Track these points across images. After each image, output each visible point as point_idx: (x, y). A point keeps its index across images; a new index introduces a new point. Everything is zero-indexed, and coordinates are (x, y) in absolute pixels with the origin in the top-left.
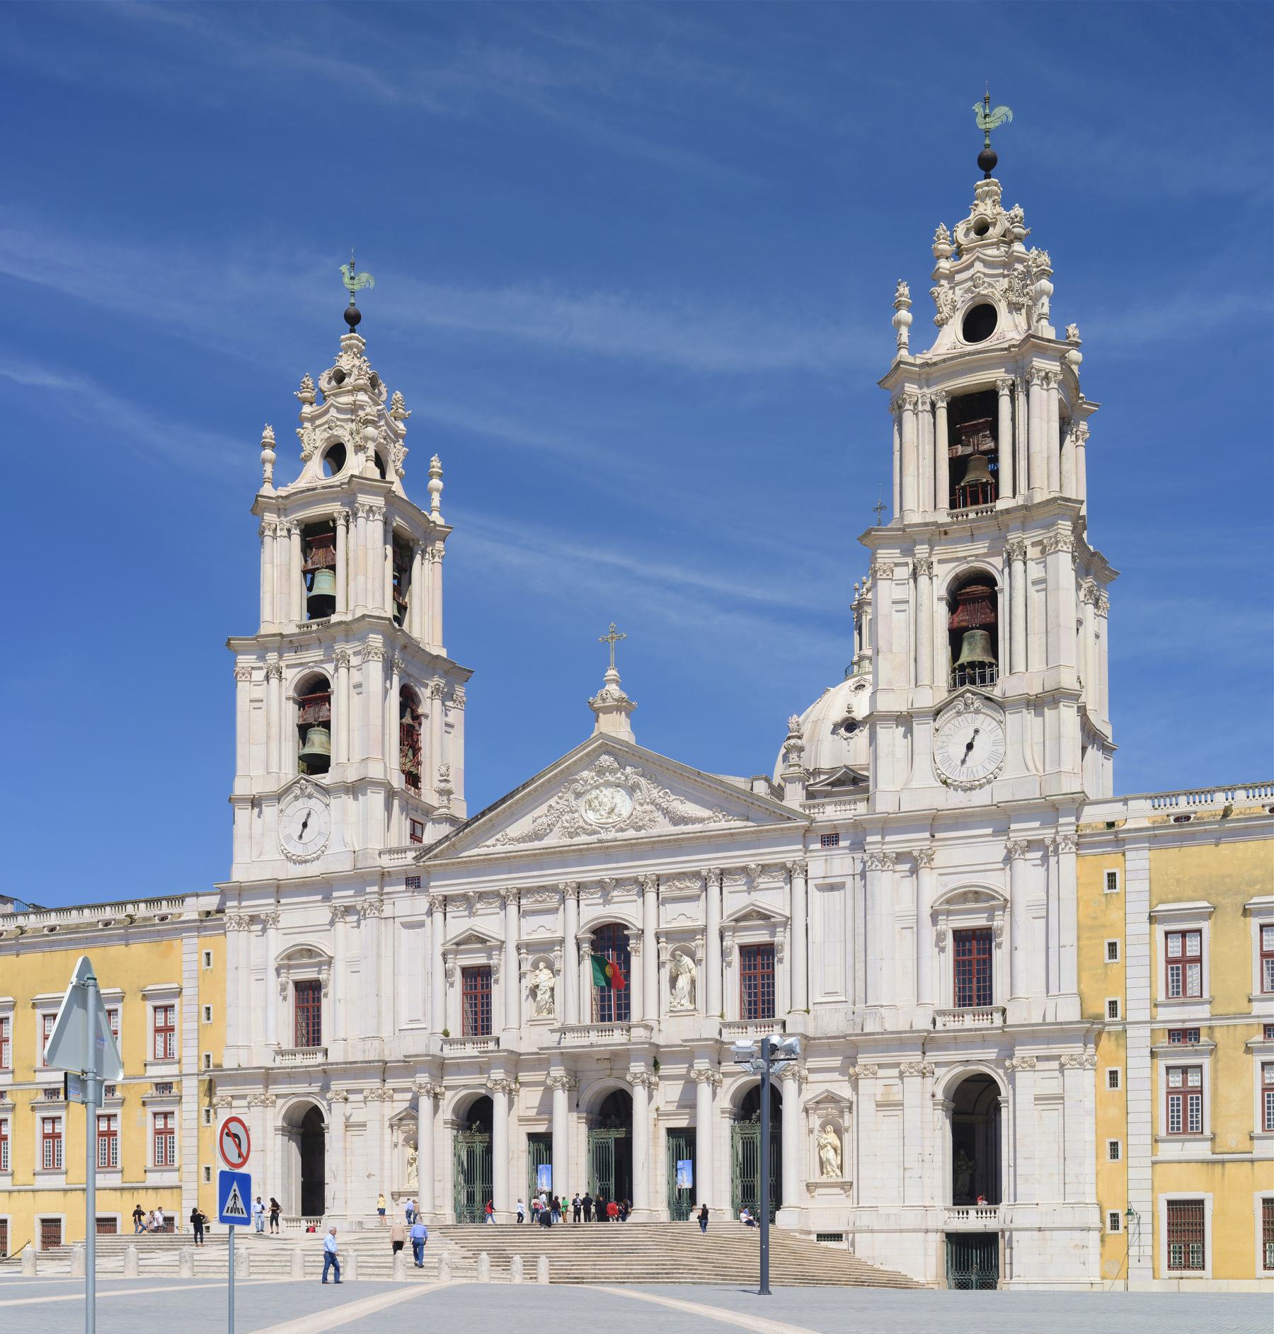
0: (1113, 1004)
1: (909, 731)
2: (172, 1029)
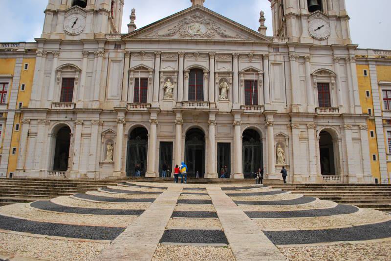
0: (370, 110)
1: (301, 19)
2: (6, 92)
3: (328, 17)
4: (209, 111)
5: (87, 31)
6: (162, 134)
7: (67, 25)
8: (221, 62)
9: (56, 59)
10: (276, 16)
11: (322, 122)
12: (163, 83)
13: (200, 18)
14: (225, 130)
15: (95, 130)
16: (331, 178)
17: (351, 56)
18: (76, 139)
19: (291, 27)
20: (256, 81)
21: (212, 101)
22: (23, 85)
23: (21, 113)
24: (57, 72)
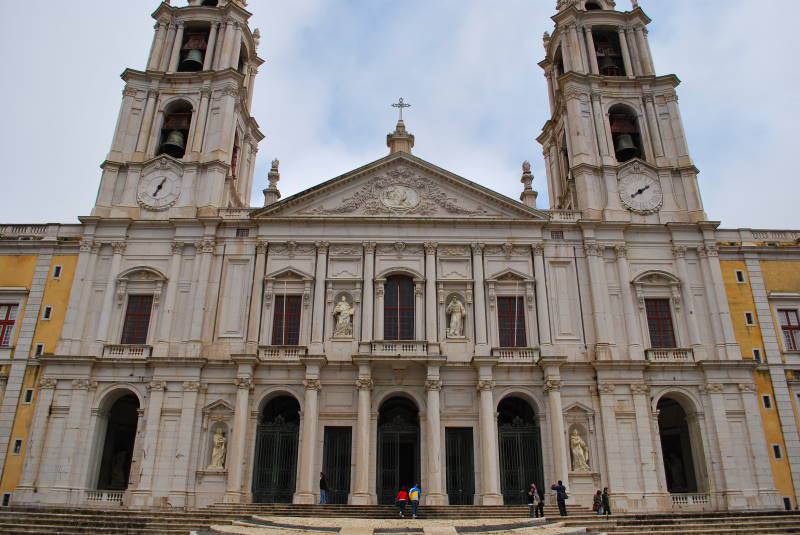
0: (756, 352)
1: (602, 176)
2: (12, 322)
3: (657, 170)
4: (427, 362)
5: (184, 202)
6: (329, 410)
7: (144, 190)
8: (448, 261)
9: (117, 257)
10: (554, 171)
11: (660, 378)
12: (332, 306)
13: (405, 176)
14: (460, 400)
15: (189, 403)
16: (690, 499)
17: (709, 244)
18: (148, 422)
19: (586, 190)
20: (521, 299)
21: (432, 339)
22: (49, 310)
23: (38, 367)
24: (118, 283)
